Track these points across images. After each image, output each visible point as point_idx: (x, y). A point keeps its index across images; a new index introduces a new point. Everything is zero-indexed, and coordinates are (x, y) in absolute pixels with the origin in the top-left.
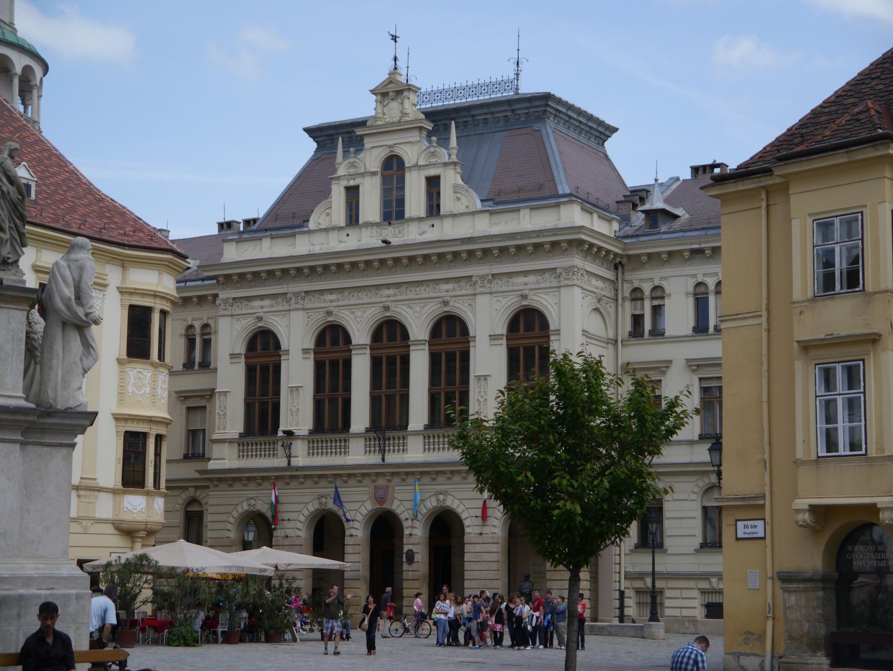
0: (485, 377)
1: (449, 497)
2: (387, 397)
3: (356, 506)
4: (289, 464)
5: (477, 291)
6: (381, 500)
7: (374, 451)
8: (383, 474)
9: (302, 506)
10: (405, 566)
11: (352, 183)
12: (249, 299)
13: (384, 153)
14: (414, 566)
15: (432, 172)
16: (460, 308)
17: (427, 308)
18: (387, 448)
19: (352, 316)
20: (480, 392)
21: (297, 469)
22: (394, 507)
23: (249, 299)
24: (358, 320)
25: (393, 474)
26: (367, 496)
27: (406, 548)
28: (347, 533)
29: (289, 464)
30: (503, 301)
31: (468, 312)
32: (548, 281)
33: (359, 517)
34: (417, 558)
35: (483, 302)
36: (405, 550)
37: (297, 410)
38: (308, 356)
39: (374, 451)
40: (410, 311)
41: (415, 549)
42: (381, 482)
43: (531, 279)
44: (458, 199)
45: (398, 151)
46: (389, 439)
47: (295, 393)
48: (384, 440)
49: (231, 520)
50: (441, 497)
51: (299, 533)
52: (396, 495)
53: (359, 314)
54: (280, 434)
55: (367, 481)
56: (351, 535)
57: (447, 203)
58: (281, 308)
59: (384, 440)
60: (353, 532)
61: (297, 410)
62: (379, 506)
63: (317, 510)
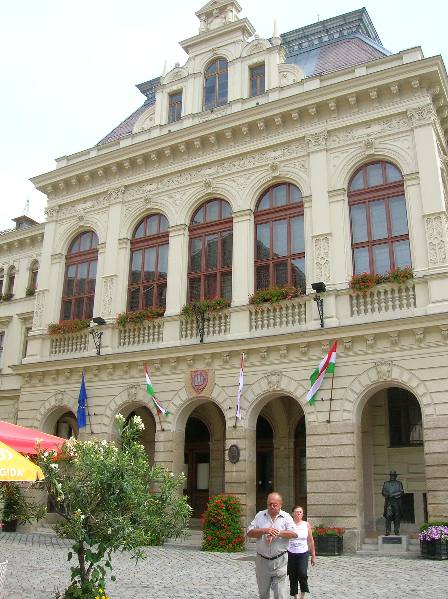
0: (326, 237)
1: (283, 378)
2: (207, 277)
3: (168, 396)
4: (98, 353)
5: (311, 150)
6: (199, 388)
7: (192, 335)
8: (201, 357)
9: (108, 400)
10: (228, 466)
11: (175, 88)
12: (73, 203)
13: (209, 57)
14: (240, 466)
15: (255, 60)
16: (290, 172)
17: (252, 178)
18: (206, 330)
19: (171, 201)
20: (319, 254)
21: (106, 357)
22: (214, 395)
23: (73, 203)
24: (177, 203)
25: (213, 356)
26: (183, 384)
27: (229, 444)
28: (158, 427)
29: (98, 353)
30: (342, 156)
31: (301, 174)
32: (398, 126)
33: (173, 409)
34: (244, 455)
35: (318, 161)
36: (228, 446)
37: (111, 300)
38: (124, 246)
39: (192, 335)
40: (234, 185)
41: (241, 444)
42: (200, 366)
43: (375, 128)
44: (285, 77)
45: (221, 53)
46: (209, 320)
47: (109, 283)
48: (204, 320)
49: (39, 417)
50: (274, 379)
51: (105, 429)
52: (216, 381)
53: (178, 196)
54: (92, 324)
55: (183, 367)
56: (163, 430)
57: (272, 79)
58: (101, 206)
59: (204, 320)
60: (165, 426)
61: (111, 300)
62: (195, 395)
63: (125, 403)
